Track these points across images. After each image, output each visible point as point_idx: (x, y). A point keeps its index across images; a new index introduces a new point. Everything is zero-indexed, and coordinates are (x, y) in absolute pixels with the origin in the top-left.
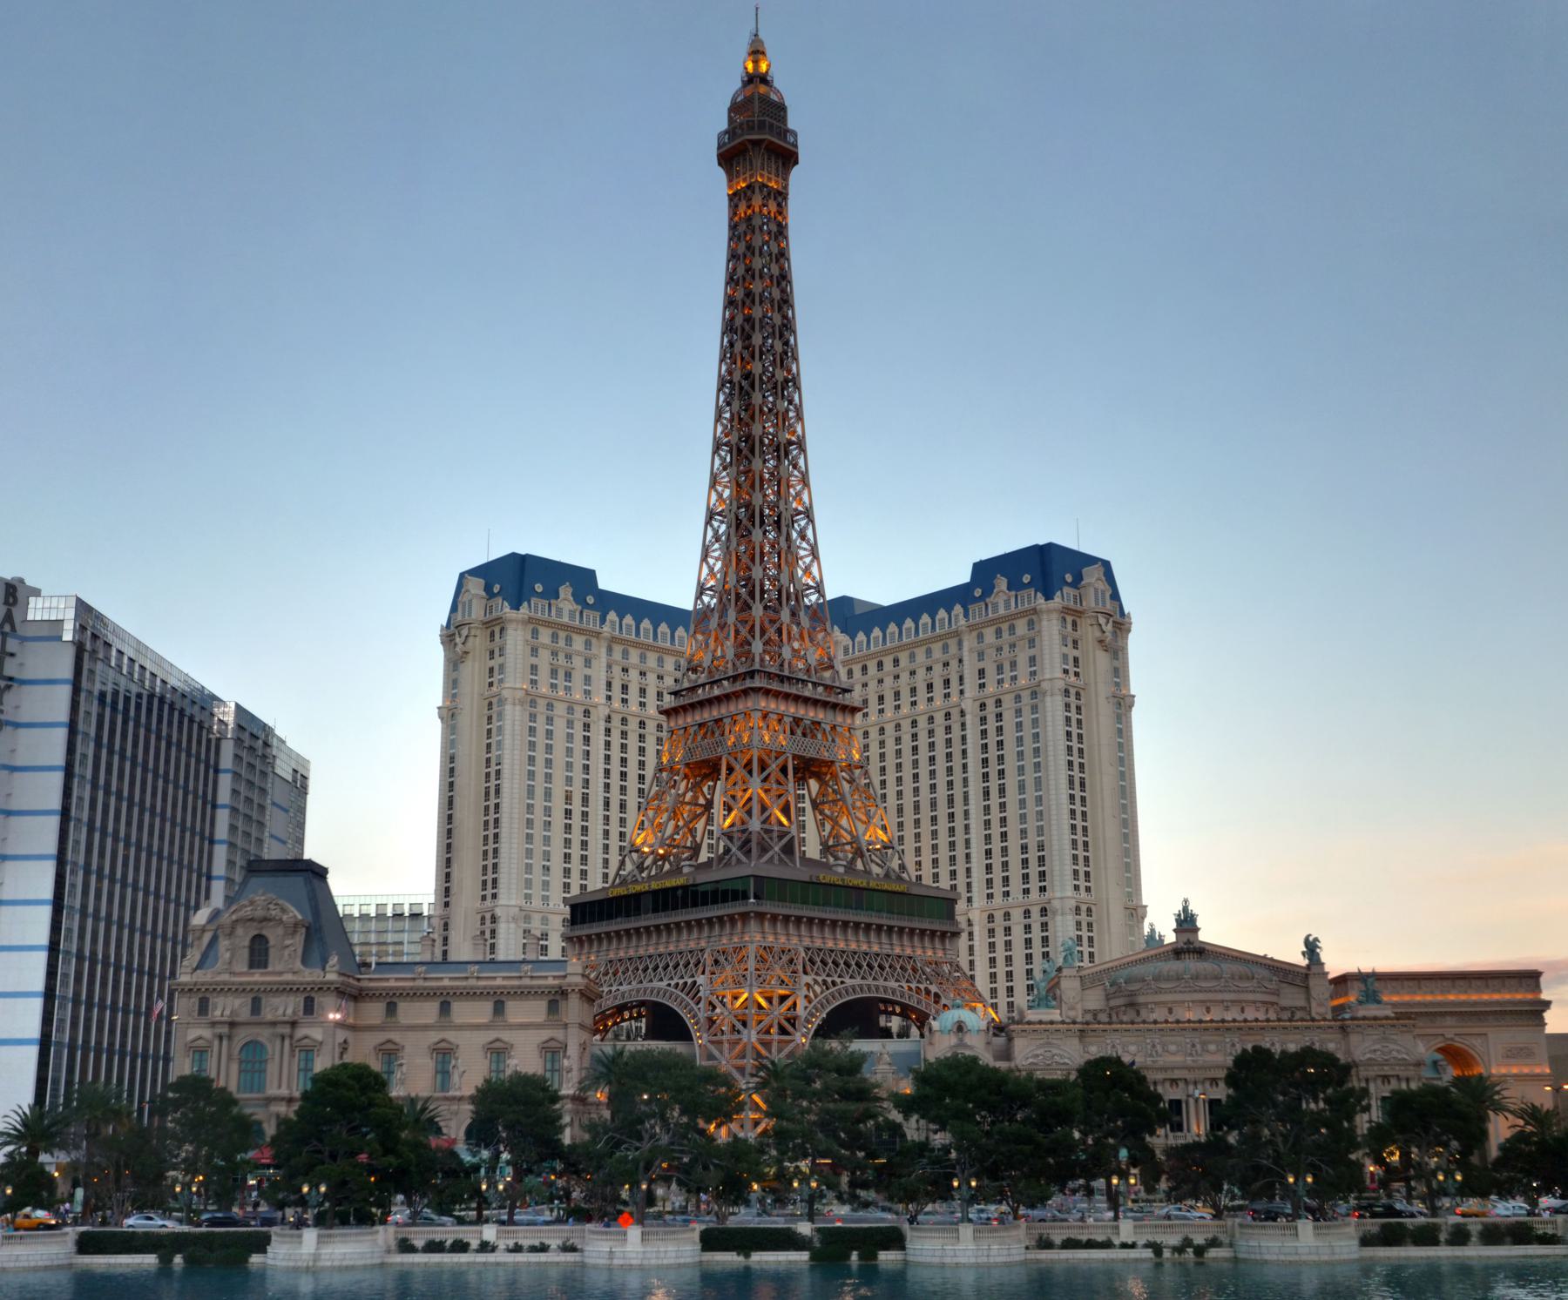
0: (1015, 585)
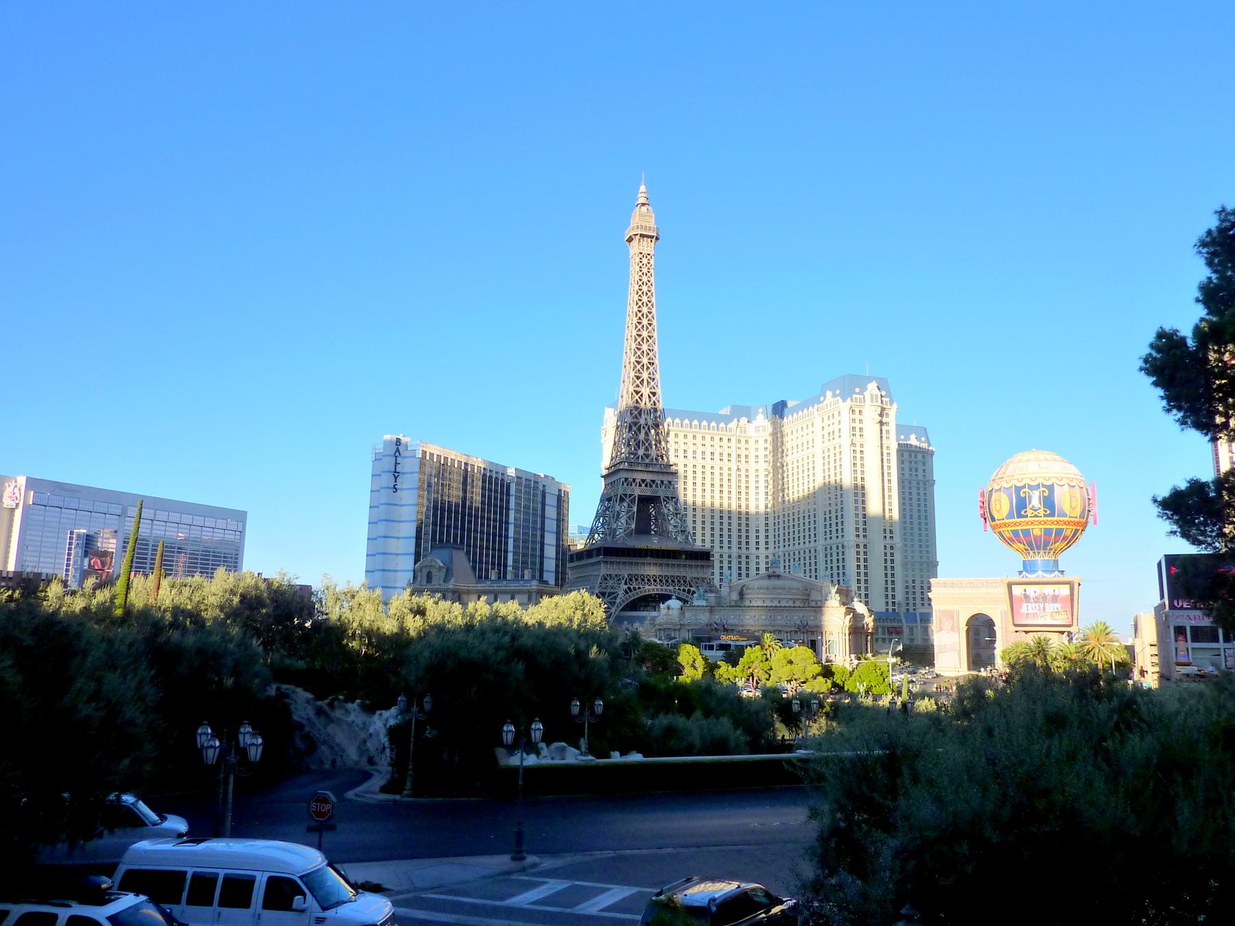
0: (834, 396)
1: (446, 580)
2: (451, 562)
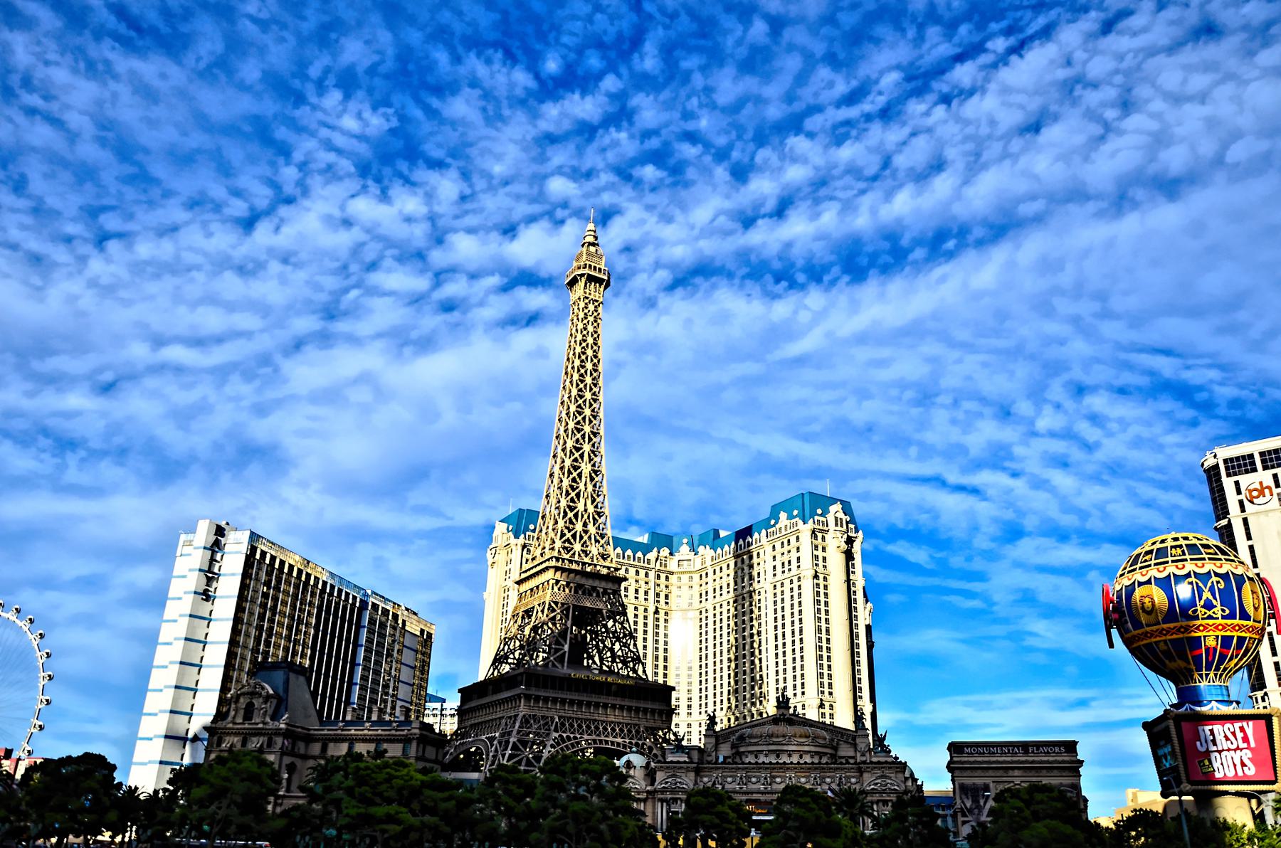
0: (790, 517)
1: (275, 717)
2: (286, 690)
